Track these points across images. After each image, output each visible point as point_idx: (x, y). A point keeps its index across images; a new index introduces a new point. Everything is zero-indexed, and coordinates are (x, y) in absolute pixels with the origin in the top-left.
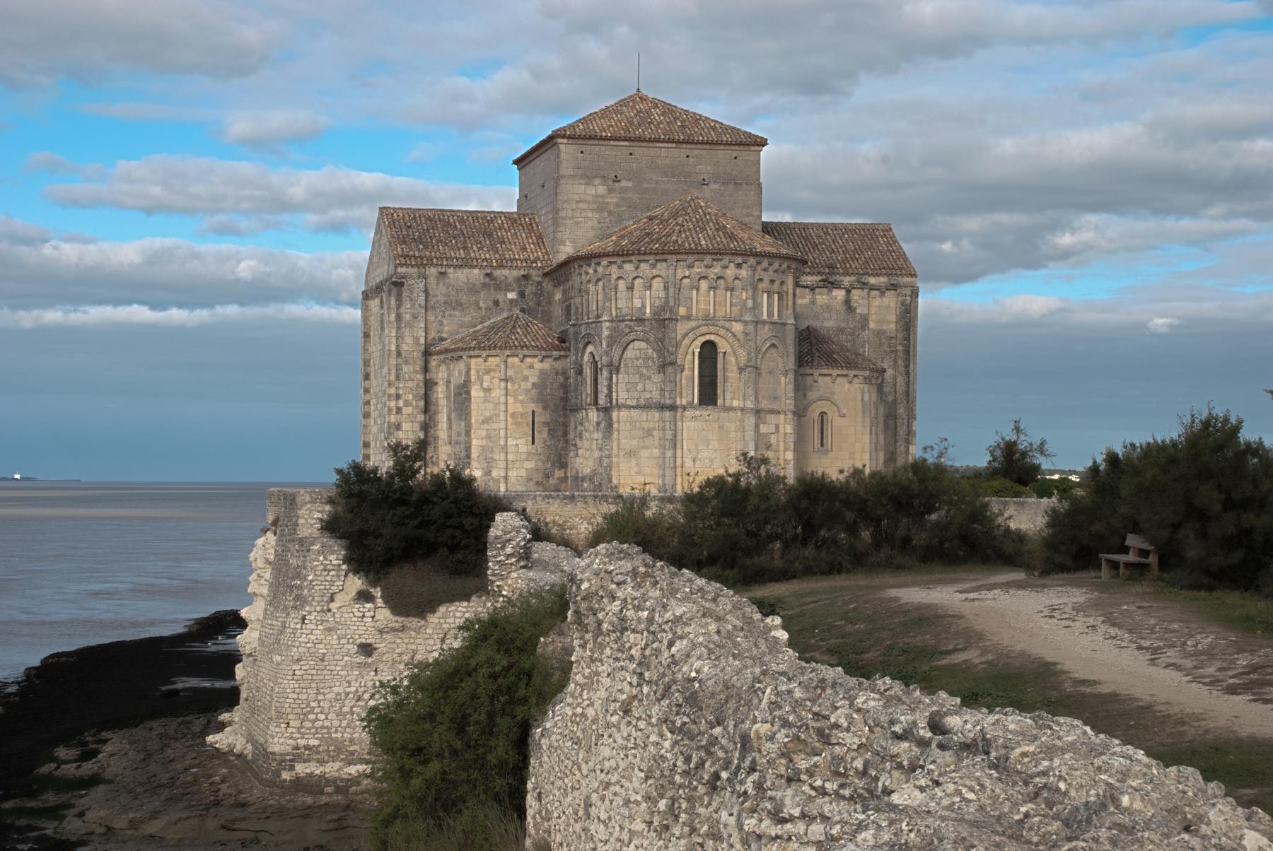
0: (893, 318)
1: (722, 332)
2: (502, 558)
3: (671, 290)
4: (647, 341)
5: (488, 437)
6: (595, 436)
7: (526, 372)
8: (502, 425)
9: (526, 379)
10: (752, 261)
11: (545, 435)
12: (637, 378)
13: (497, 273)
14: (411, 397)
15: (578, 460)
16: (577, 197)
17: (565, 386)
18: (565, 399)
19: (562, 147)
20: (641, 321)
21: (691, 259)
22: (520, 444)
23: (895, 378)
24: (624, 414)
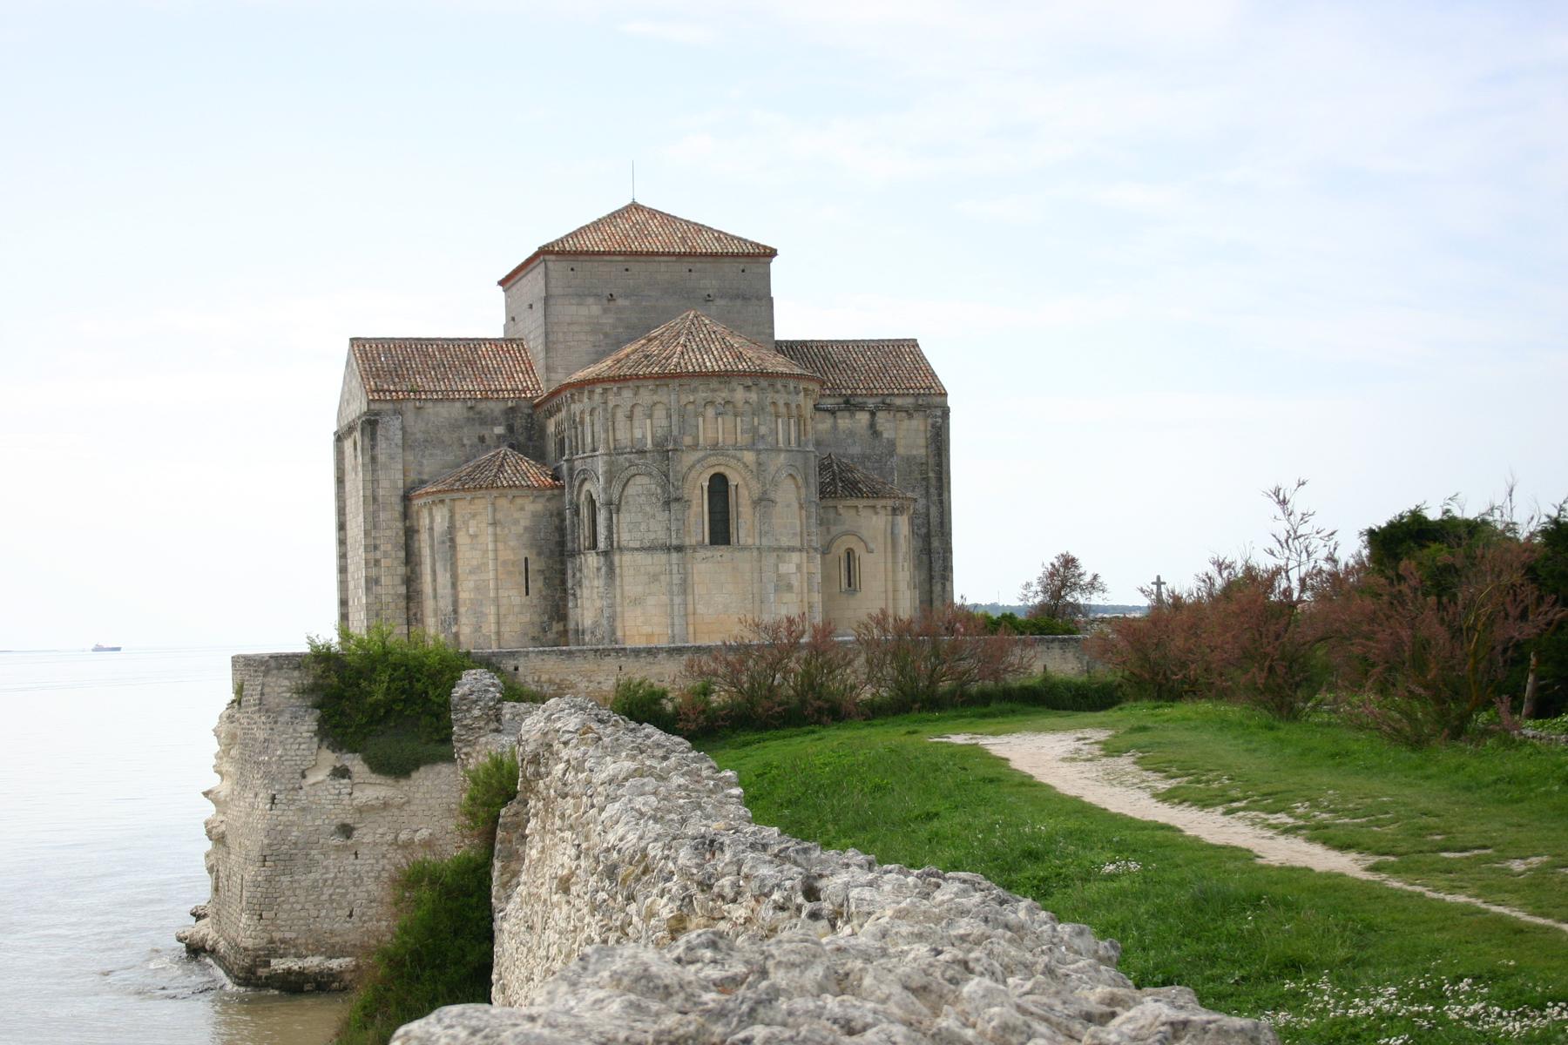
0: (922, 442)
1: (733, 462)
2: (469, 721)
3: (675, 418)
5: (477, 589)
6: (596, 583)
8: (492, 575)
9: (516, 522)
10: (764, 383)
11: (540, 584)
13: (482, 406)
14: (389, 547)
15: (579, 611)
17: (561, 530)
18: (562, 544)
19: (550, 265)
20: (642, 452)
21: (695, 383)
22: (513, 596)
23: (928, 508)
24: (627, 558)
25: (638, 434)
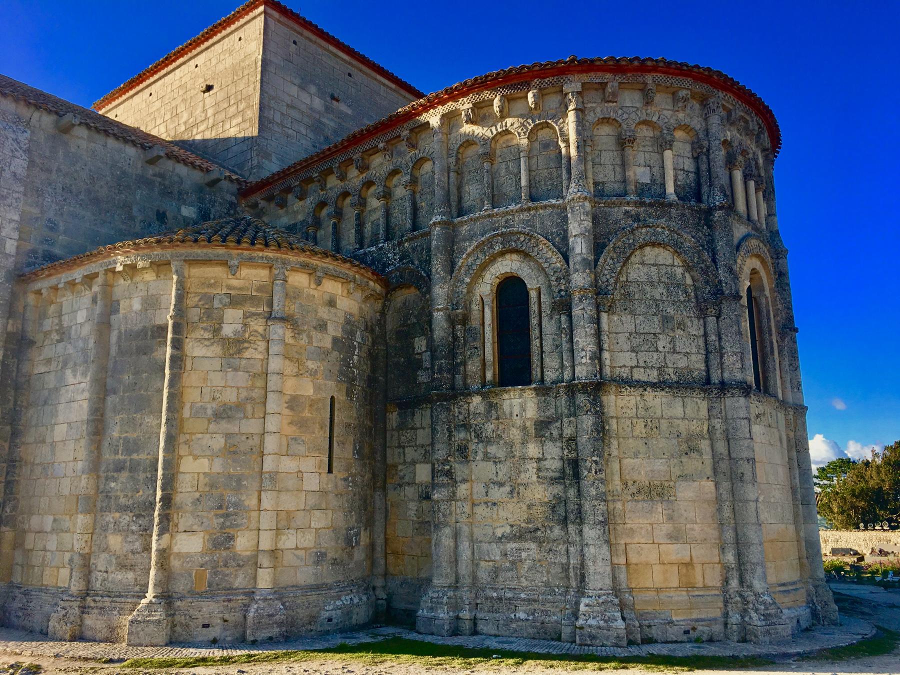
4: (677, 249)
7: (324, 313)
9: (322, 326)
12: (655, 325)
16: (288, 100)
25: (640, 174)
